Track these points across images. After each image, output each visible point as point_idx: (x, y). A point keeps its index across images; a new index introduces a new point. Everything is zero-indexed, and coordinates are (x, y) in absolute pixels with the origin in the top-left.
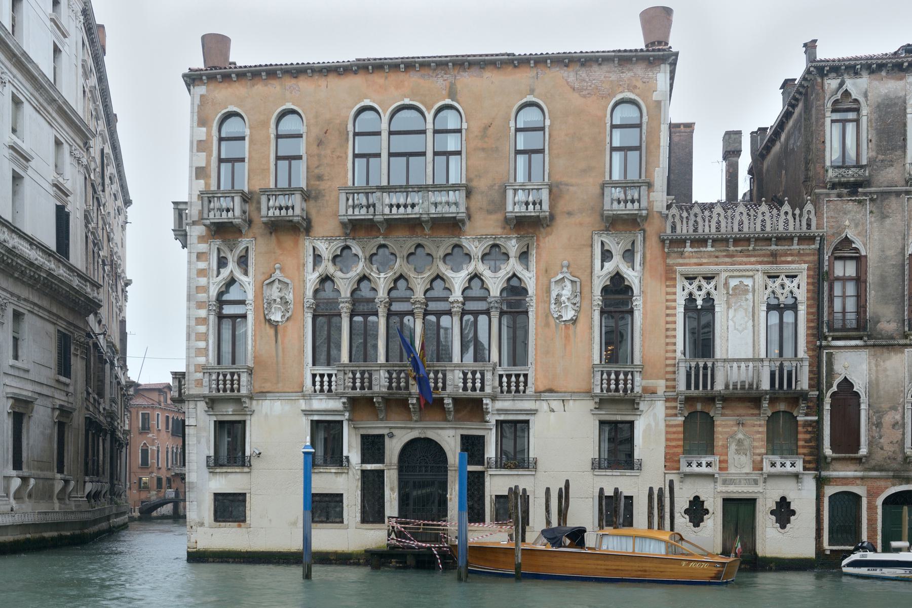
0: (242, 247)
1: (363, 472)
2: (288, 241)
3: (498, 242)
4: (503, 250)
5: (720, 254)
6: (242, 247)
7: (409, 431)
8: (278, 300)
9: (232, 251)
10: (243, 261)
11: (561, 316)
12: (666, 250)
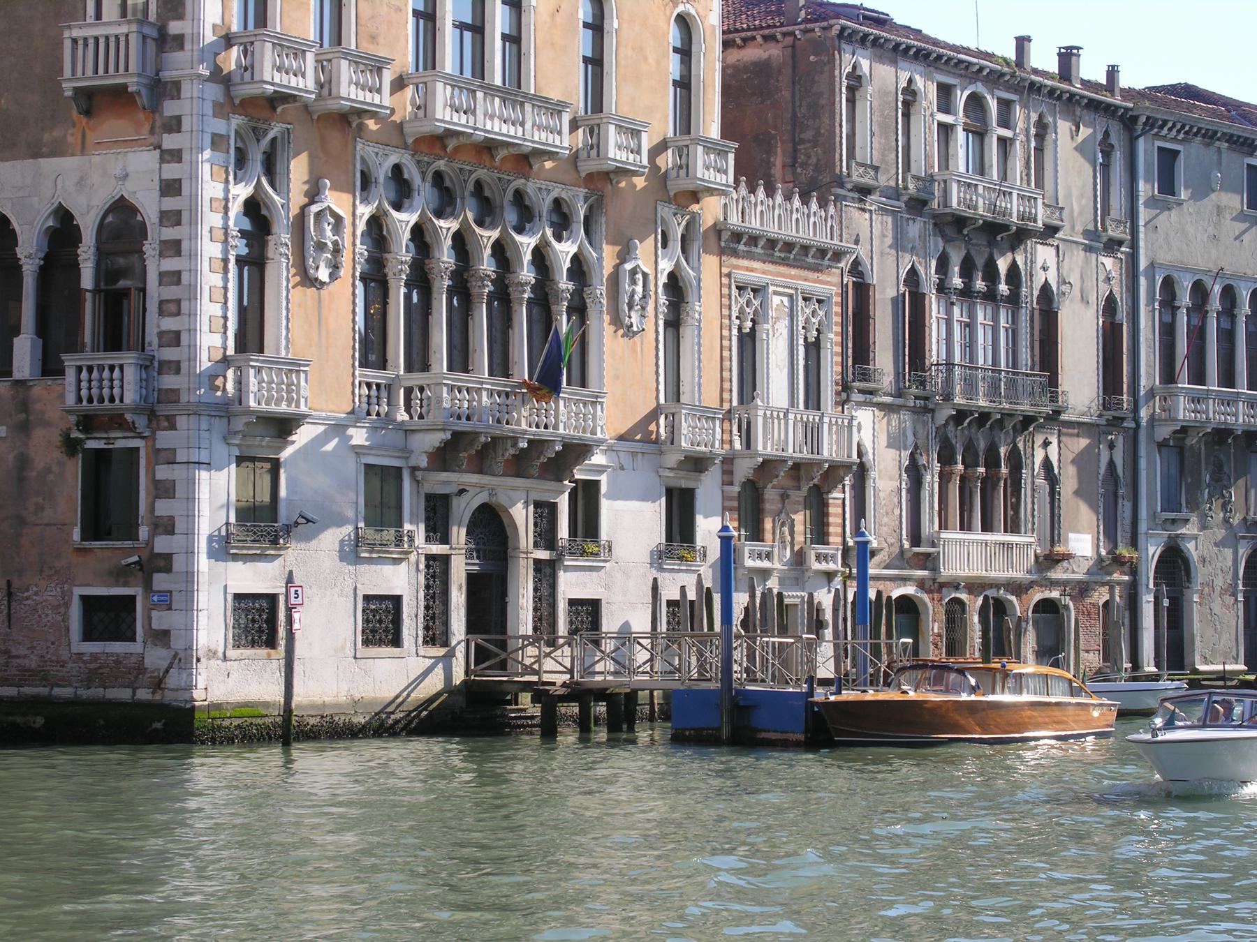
0: (271, 135)
1: (430, 558)
2: (335, 138)
3: (564, 195)
4: (565, 210)
5: (765, 258)
6: (271, 135)
7: (478, 490)
8: (330, 244)
9: (258, 140)
10: (270, 167)
11: (632, 325)
12: (723, 244)
